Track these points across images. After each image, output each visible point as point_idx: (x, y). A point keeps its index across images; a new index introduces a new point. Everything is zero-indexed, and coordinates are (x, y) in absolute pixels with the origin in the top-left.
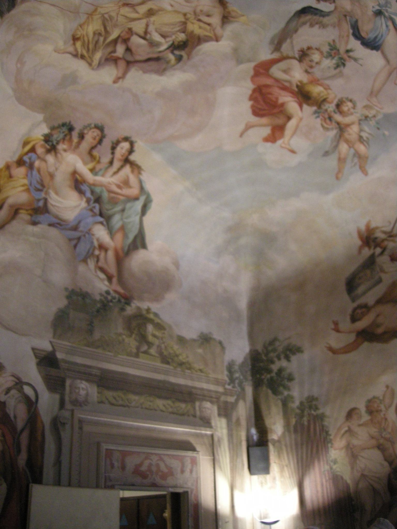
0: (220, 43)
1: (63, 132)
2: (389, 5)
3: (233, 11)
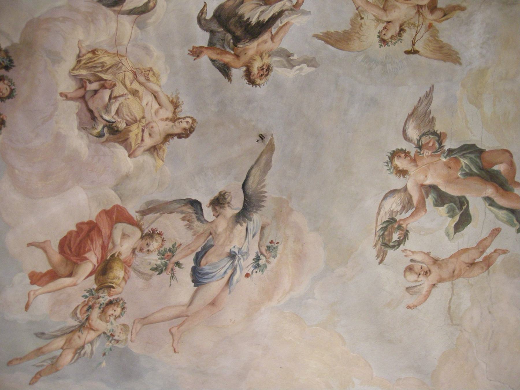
0: (128, 159)
1: (3, 61)
2: (245, 257)
3: (164, 151)
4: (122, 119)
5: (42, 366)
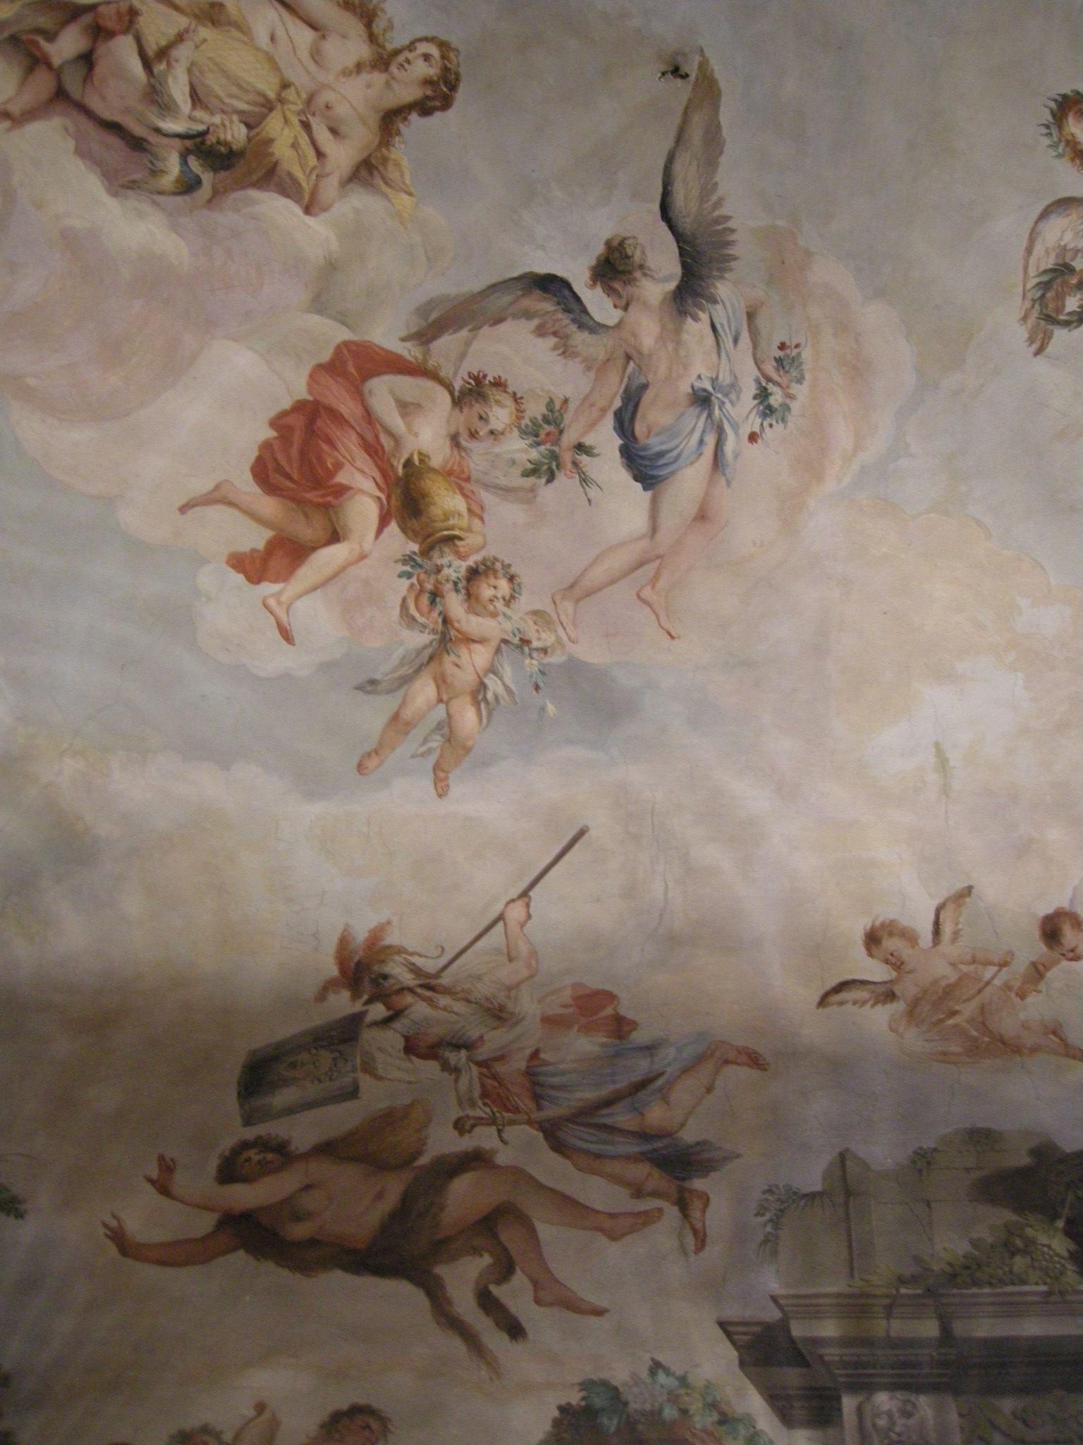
0: (309, 220)
2: (733, 396)
3: (397, 165)
4: (223, 112)
5: (430, 751)
